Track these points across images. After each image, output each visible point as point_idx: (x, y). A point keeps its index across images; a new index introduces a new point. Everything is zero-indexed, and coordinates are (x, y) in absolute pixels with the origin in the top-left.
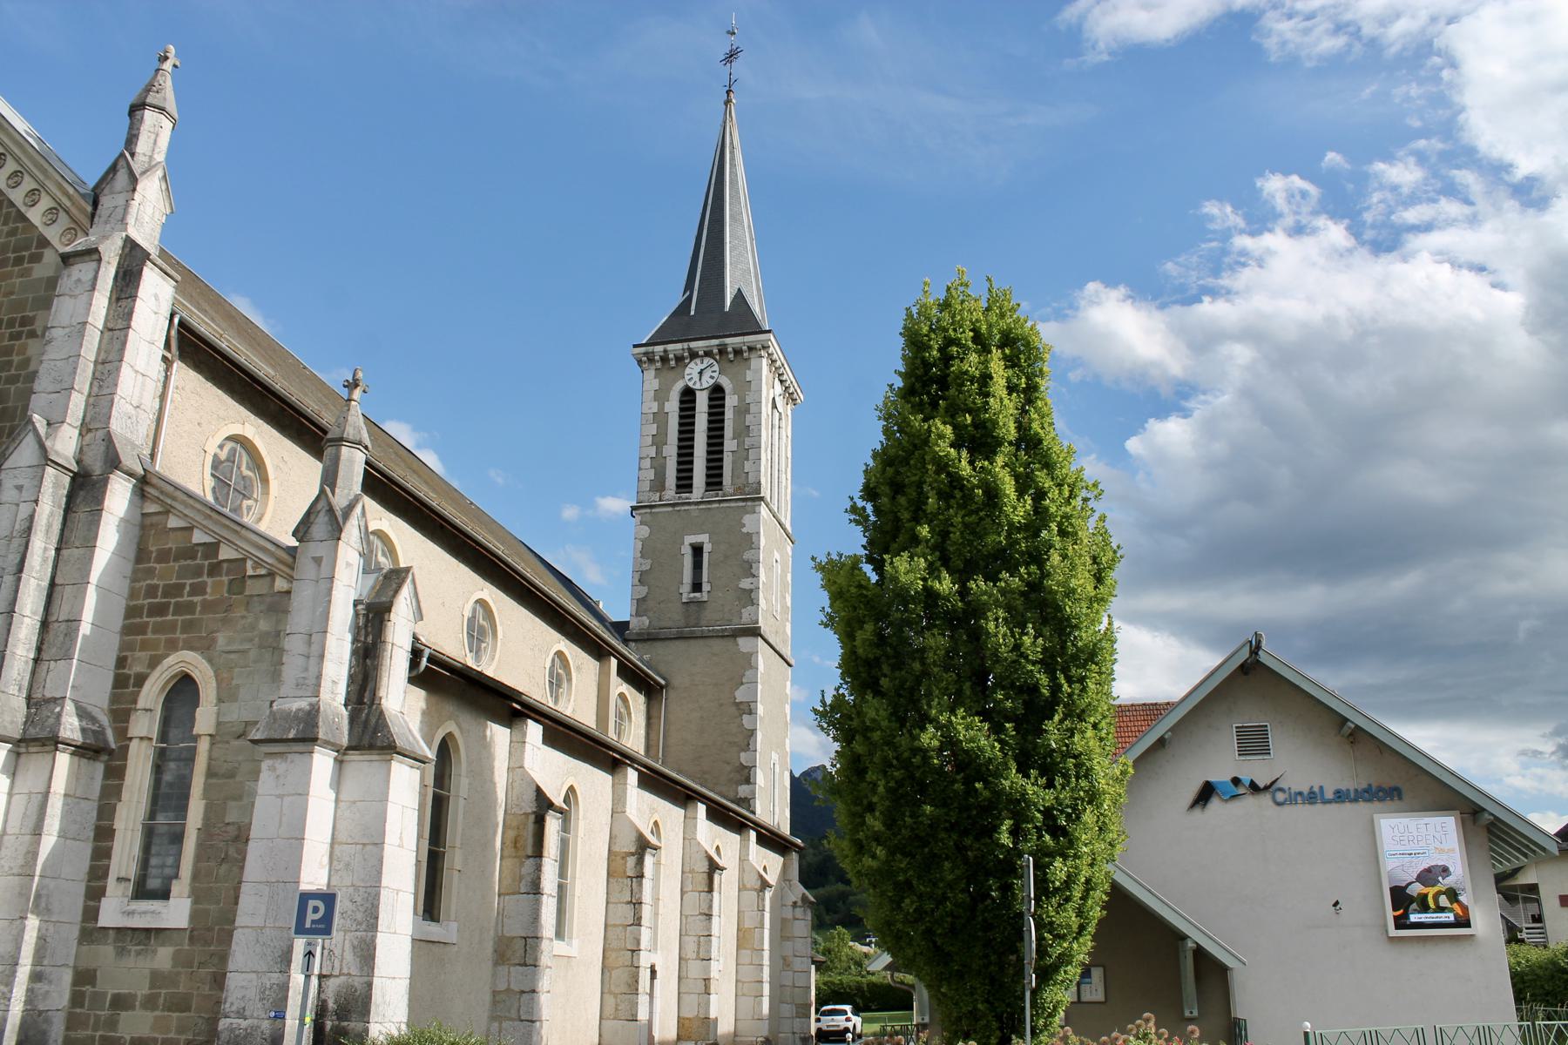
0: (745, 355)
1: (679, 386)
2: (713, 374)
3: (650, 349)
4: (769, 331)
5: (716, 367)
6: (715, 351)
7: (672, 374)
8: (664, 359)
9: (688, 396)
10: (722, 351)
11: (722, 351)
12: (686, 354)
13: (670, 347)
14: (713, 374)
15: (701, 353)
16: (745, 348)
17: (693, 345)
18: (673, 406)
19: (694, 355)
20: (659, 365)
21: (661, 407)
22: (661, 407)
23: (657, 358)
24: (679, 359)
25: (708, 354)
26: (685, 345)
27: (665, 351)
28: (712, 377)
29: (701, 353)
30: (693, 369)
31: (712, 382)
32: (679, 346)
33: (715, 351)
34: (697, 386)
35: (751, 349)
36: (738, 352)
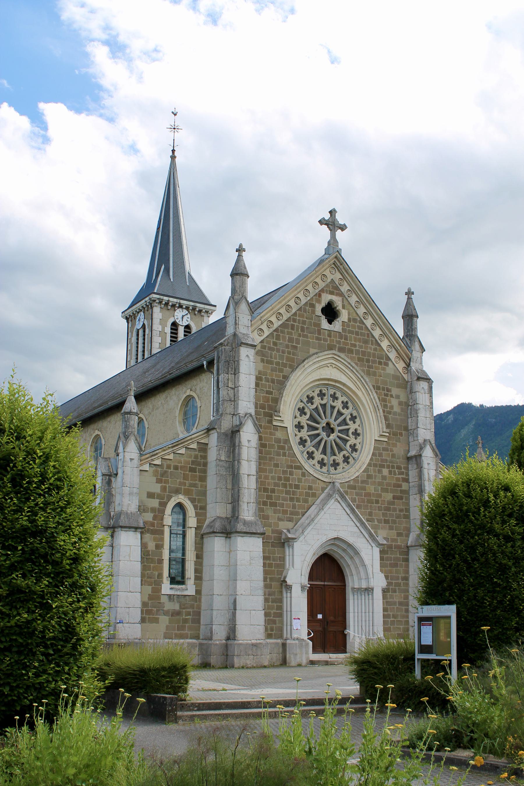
0: (203, 314)
1: (171, 320)
2: (188, 319)
3: (162, 297)
4: (215, 306)
5: (189, 316)
6: (191, 308)
7: (167, 313)
8: (167, 304)
9: (175, 325)
10: (194, 309)
11: (194, 309)
12: (177, 305)
13: (171, 299)
14: (188, 319)
15: (184, 307)
16: (204, 311)
17: (182, 302)
18: (168, 330)
19: (181, 306)
20: (163, 306)
21: (163, 329)
22: (163, 329)
23: (164, 303)
24: (173, 306)
25: (187, 308)
26: (178, 301)
27: (168, 301)
28: (188, 321)
29: (184, 307)
30: (179, 314)
31: (187, 323)
32: (175, 300)
33: (191, 308)
34: (180, 323)
35: (207, 312)
36: (200, 311)
